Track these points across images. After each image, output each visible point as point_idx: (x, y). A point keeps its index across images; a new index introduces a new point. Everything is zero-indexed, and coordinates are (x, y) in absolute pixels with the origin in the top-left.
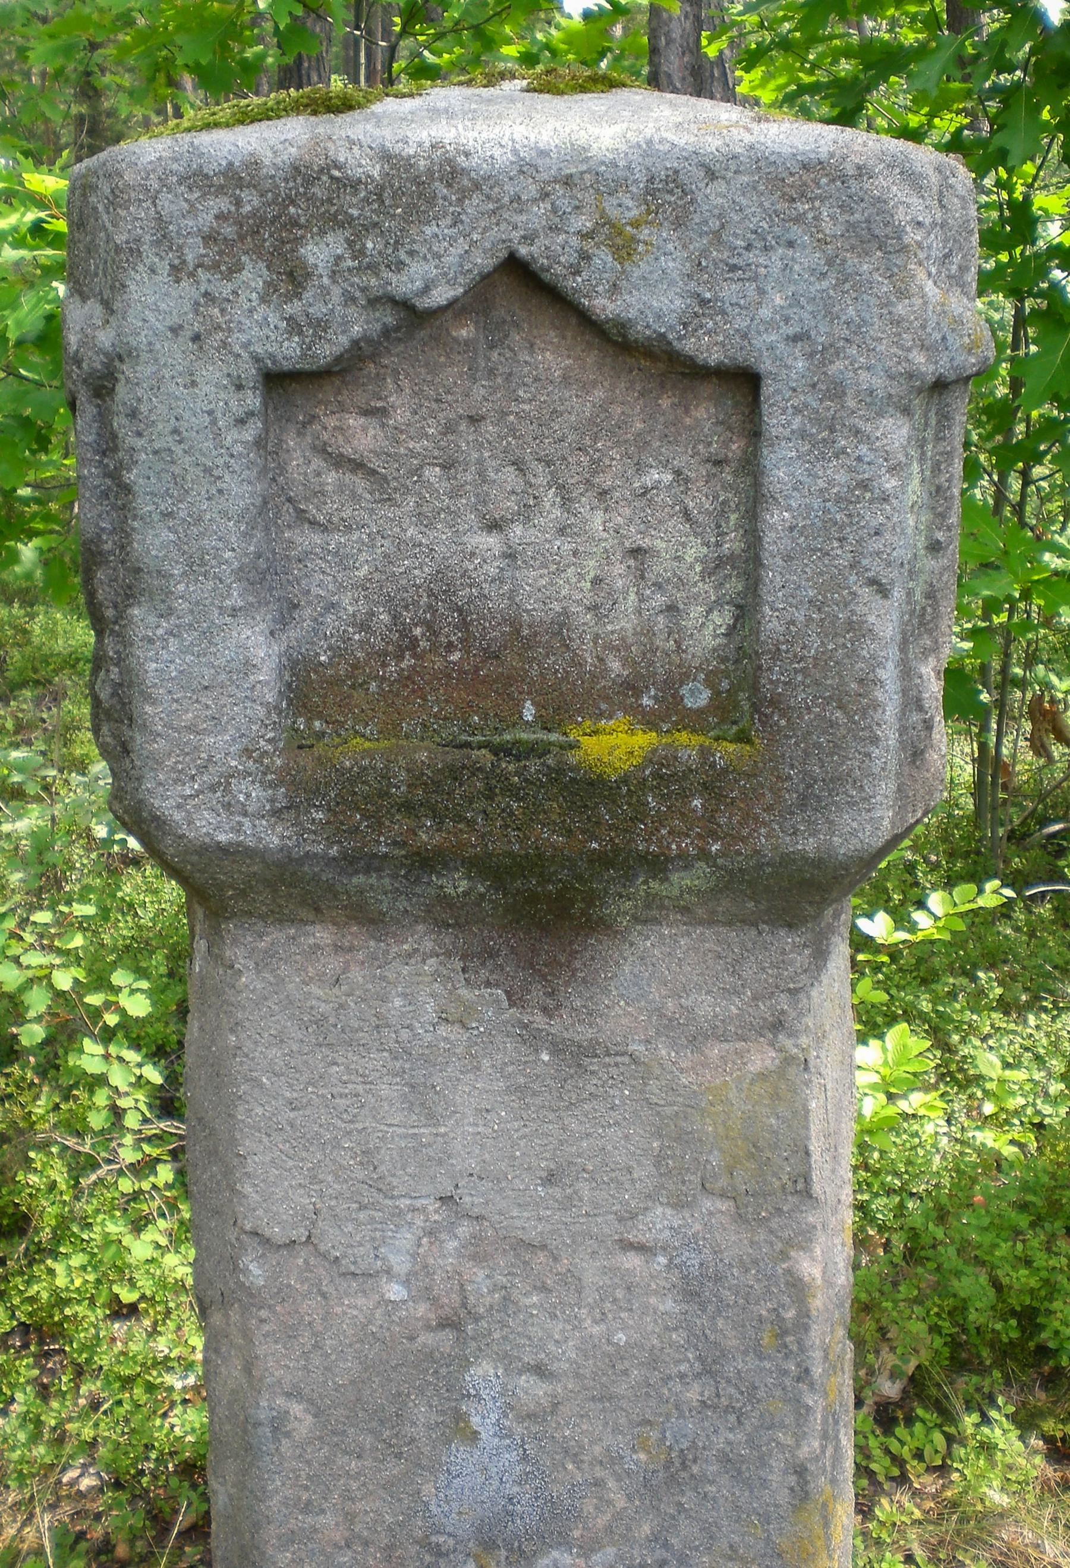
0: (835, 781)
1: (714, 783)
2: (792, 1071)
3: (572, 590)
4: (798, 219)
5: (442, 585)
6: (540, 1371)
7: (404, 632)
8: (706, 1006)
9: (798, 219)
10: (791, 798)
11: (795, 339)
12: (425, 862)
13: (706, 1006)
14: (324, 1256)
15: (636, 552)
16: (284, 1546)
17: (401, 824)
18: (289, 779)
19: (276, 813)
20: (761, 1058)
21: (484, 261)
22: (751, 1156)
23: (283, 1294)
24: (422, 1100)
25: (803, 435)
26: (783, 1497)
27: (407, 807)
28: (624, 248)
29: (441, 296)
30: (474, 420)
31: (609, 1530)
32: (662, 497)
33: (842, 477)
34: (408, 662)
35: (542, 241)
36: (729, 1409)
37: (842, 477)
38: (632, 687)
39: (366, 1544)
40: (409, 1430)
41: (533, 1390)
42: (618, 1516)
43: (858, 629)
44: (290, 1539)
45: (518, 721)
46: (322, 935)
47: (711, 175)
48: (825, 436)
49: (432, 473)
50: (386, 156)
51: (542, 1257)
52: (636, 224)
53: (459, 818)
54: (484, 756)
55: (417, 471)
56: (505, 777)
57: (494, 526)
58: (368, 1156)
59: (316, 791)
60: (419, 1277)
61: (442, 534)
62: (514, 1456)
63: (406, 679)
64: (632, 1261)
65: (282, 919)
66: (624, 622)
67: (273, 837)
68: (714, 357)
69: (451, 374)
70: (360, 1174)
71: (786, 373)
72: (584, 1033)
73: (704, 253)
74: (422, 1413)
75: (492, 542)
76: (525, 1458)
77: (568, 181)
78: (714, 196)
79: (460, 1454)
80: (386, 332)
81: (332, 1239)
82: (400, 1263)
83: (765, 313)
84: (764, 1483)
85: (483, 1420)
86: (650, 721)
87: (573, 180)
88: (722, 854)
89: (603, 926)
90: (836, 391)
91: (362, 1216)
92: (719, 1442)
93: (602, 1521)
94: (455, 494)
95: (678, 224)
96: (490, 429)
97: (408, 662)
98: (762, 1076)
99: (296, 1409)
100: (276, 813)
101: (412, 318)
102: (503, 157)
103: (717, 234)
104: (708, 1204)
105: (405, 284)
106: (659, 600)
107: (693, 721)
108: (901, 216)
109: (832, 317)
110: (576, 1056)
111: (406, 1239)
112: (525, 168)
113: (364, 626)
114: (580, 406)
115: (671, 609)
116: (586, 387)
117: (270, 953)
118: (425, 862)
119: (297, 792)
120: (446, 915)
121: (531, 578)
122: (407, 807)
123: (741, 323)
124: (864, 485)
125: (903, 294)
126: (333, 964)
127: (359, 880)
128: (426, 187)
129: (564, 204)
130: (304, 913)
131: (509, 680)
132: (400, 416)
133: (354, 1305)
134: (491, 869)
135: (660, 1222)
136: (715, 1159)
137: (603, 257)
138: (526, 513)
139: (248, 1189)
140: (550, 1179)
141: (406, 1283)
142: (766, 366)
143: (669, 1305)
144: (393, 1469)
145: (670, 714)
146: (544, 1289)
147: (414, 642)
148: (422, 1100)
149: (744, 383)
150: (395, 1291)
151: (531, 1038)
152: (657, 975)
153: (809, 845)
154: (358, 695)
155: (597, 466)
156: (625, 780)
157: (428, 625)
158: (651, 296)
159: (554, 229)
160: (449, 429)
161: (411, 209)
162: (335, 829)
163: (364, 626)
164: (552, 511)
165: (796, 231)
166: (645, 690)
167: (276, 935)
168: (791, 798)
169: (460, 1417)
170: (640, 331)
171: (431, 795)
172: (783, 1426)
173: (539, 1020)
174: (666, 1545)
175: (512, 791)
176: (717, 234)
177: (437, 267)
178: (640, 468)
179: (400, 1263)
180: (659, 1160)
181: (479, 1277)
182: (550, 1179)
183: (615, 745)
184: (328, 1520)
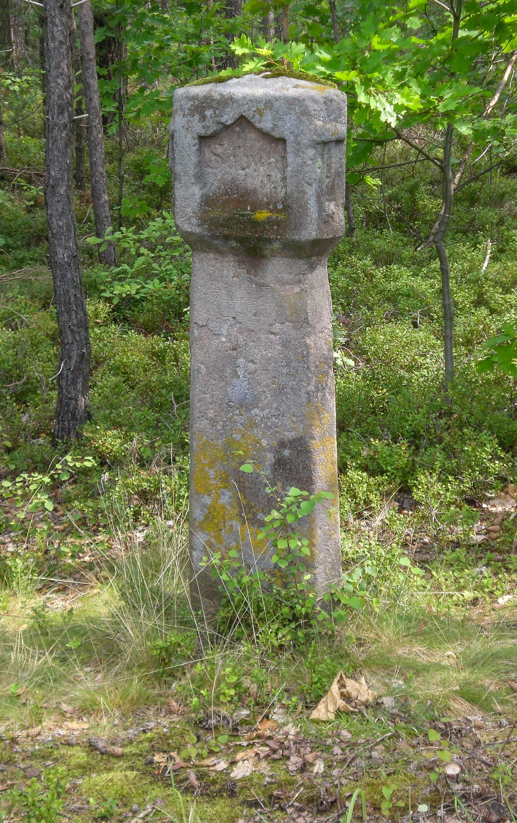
0: (301, 224)
1: (278, 223)
2: (303, 292)
3: (257, 183)
4: (292, 109)
5: (234, 181)
6: (252, 361)
7: (227, 190)
8: (286, 276)
9: (292, 109)
10: (293, 227)
11: (292, 133)
12: (227, 238)
13: (286, 276)
14: (209, 329)
15: (269, 175)
16: (198, 402)
17: (221, 229)
18: (201, 218)
19: (199, 225)
20: (297, 289)
21: (237, 116)
22: (295, 313)
23: (201, 338)
24: (230, 294)
25: (293, 152)
26: (304, 400)
27: (222, 225)
28: (261, 115)
29: (229, 122)
30: (239, 147)
31: (267, 404)
32: (273, 164)
33: (300, 161)
34: (227, 196)
35: (247, 112)
36: (293, 375)
37: (300, 161)
38: (268, 204)
39: (216, 403)
40: (225, 374)
41: (252, 366)
42: (269, 401)
43: (305, 193)
44: (200, 400)
45: (247, 210)
46: (211, 255)
47: (277, 100)
48: (297, 152)
49: (232, 158)
50: (221, 94)
51: (253, 333)
52: (263, 109)
53: (232, 228)
54: (237, 216)
55: (229, 157)
56: (240, 220)
57: (243, 169)
58: (219, 307)
59: (206, 221)
60: (228, 335)
61: (233, 170)
62: (247, 382)
63: (226, 200)
64: (272, 336)
65: (204, 251)
66: (267, 190)
67: (198, 230)
68: (277, 136)
69: (235, 138)
70: (217, 310)
71: (290, 139)
72: (262, 281)
73: (275, 115)
74: (228, 370)
75: (243, 172)
76: (249, 384)
77: (251, 101)
78: (277, 104)
79: (235, 381)
80: (221, 129)
81: (211, 325)
82: (225, 332)
83: (286, 127)
84: (300, 396)
85: (241, 372)
86: (271, 211)
87: (253, 101)
88: (280, 238)
89: (264, 257)
90: (299, 144)
91: (217, 320)
92: (290, 383)
93: (266, 402)
94: (235, 162)
95: (271, 109)
96: (242, 149)
97: (227, 196)
98: (297, 293)
99: (203, 366)
100: (199, 225)
101: (226, 127)
102: (240, 95)
103: (277, 112)
104: (287, 323)
105: (223, 120)
106: (273, 186)
107: (279, 212)
108: (310, 108)
109: (298, 128)
110: (261, 286)
111: (226, 326)
112: (244, 98)
113: (219, 189)
114: (258, 145)
115: (275, 187)
116: (259, 141)
117: (202, 259)
118: (227, 238)
119: (203, 221)
120: (234, 252)
121: (249, 180)
122: (222, 225)
123: (282, 130)
124: (305, 163)
125: (311, 124)
126: (214, 262)
127: (215, 241)
128: (227, 101)
129: (251, 105)
130: (208, 250)
131: (246, 201)
132: (226, 146)
133: (216, 342)
134: (241, 240)
135: (277, 327)
136: (288, 313)
137: (257, 116)
138: (248, 167)
139: (195, 312)
140: (255, 315)
141: (226, 337)
142: (287, 138)
143: (279, 348)
144: (222, 384)
145: (275, 210)
146: (254, 341)
147: (228, 192)
148: (230, 294)
149: (283, 141)
150: (224, 339)
151: (251, 281)
152: (277, 269)
153: (296, 238)
154: (218, 203)
155: (261, 158)
156: (262, 222)
157: (231, 189)
158: (266, 124)
159: (249, 110)
160: (234, 149)
161: (224, 105)
162: (209, 229)
163: (219, 189)
164: (253, 166)
165: (291, 112)
166: (270, 204)
167: (203, 255)
168: (293, 227)
169: (236, 372)
170: (264, 131)
171: (227, 223)
172: (304, 381)
173: (253, 278)
174: (279, 410)
175: (241, 223)
176: (277, 112)
177: (228, 118)
178: (269, 158)
179: (225, 332)
180: (277, 312)
181: (241, 338)
182: (255, 315)
183: (262, 215)
184: (208, 396)
